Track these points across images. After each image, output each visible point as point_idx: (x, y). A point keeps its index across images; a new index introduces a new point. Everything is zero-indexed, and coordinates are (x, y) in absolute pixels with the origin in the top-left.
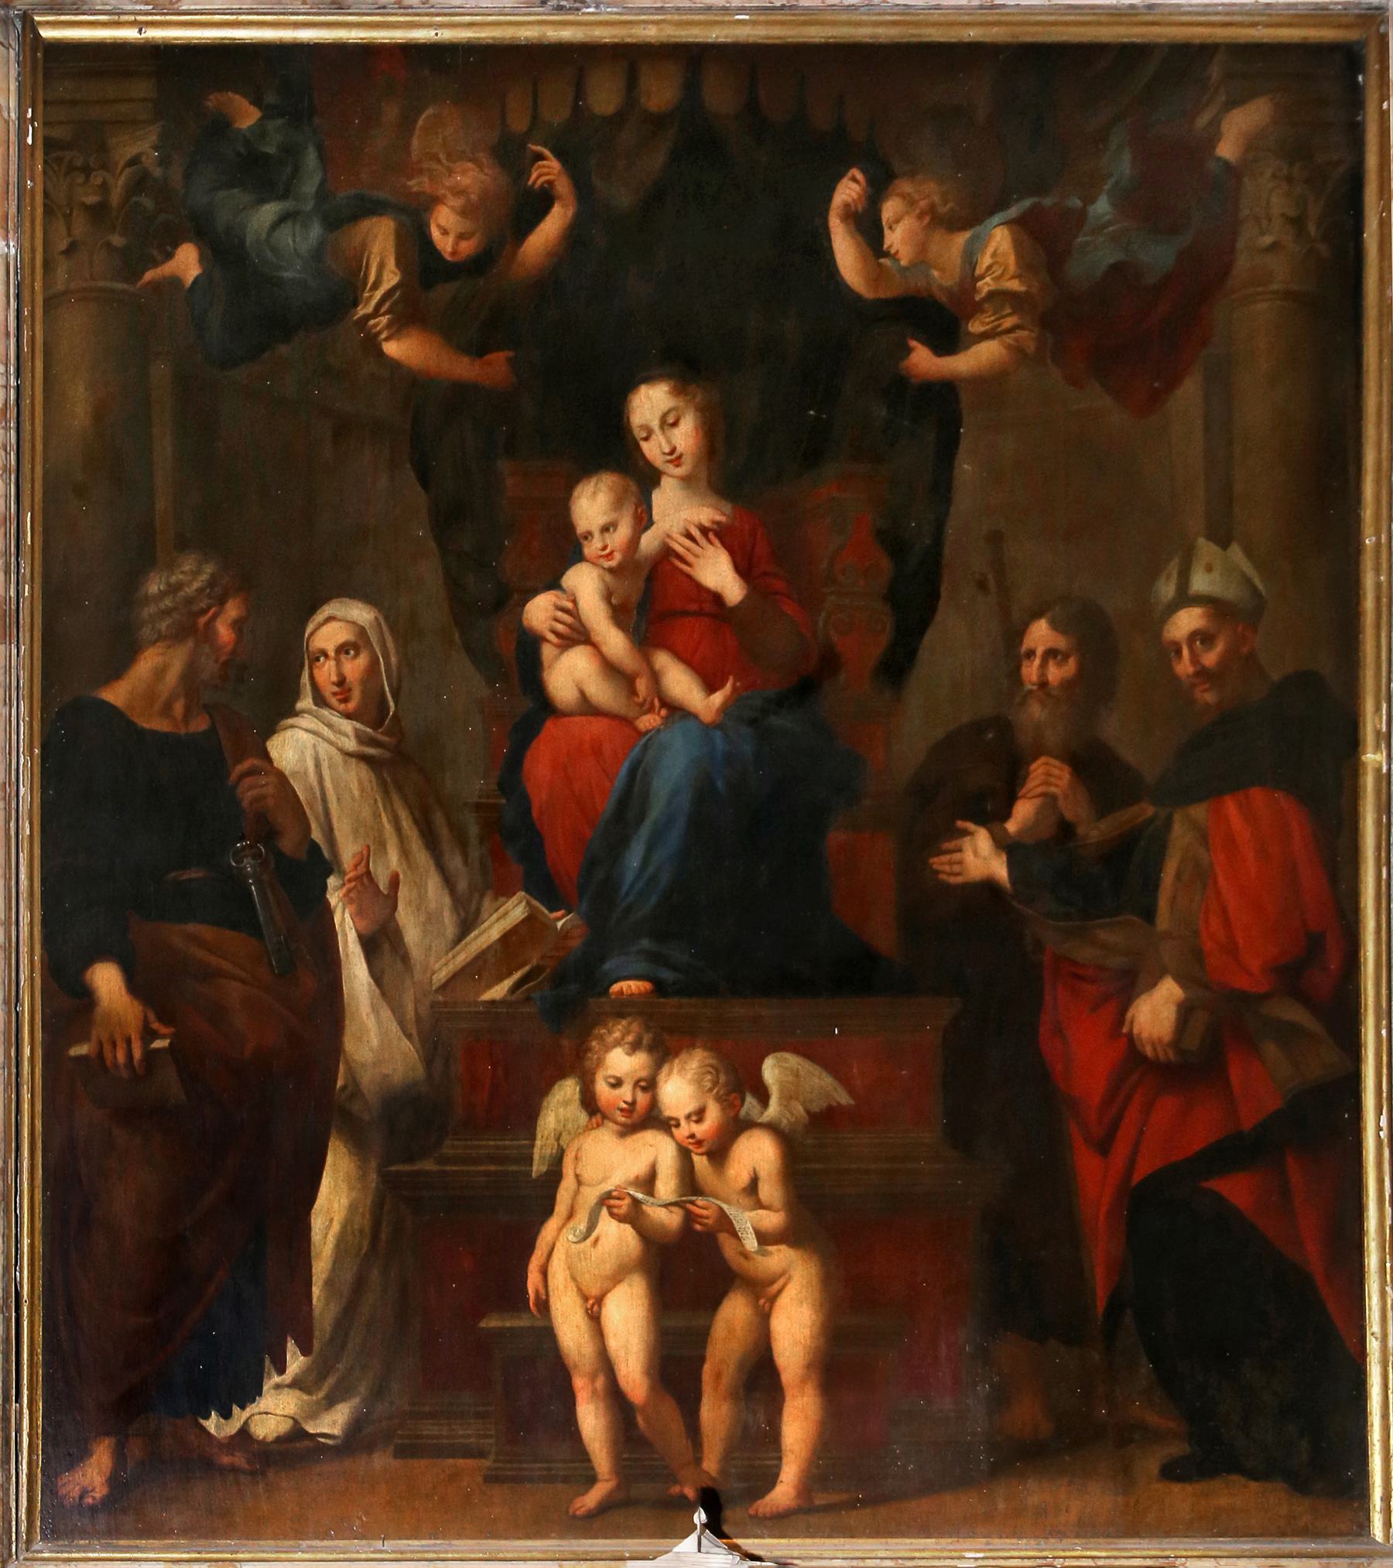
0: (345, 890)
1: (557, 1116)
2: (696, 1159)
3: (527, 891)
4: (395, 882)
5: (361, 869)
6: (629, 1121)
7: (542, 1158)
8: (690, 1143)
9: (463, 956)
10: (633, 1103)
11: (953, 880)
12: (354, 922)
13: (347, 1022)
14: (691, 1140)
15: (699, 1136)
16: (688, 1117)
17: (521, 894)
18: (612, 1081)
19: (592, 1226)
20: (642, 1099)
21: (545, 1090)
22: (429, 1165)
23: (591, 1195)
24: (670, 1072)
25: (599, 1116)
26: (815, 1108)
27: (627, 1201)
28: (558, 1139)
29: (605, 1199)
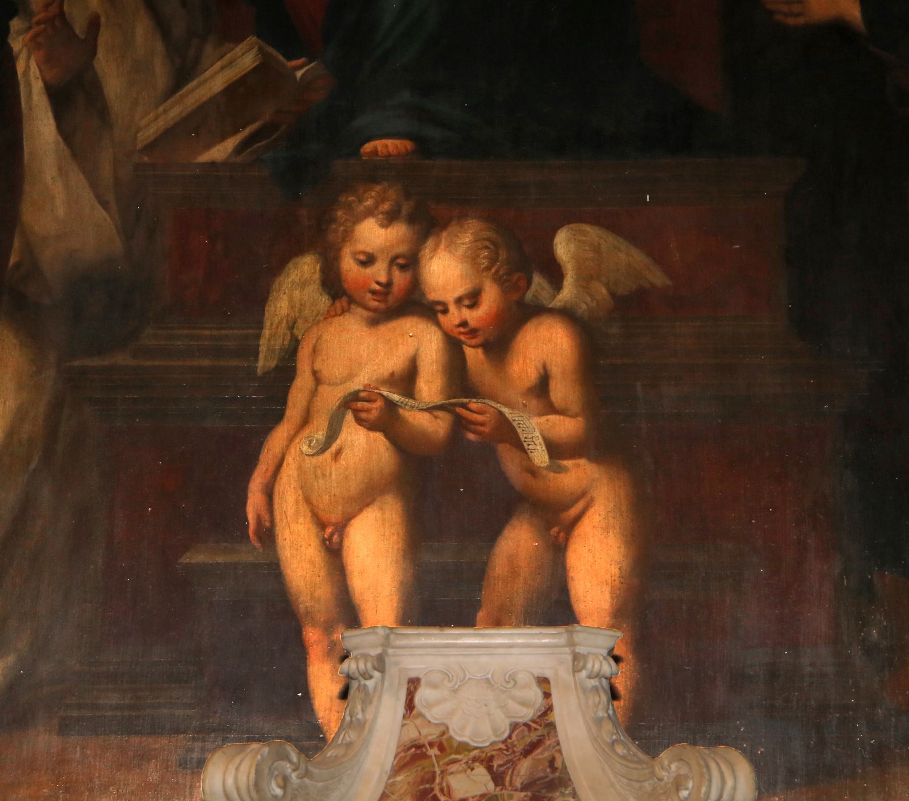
0: (31, 33)
1: (291, 300)
2: (469, 352)
3: (259, 37)
4: (94, 24)
5: (53, 9)
6: (382, 306)
7: (271, 350)
8: (461, 333)
9: (175, 111)
10: (388, 285)
11: (791, 21)
12: (40, 70)
13: (27, 188)
14: (462, 330)
15: (472, 323)
16: (459, 301)
17: (252, 39)
18: (362, 257)
19: (333, 433)
20: (400, 279)
21: (279, 266)
22: (122, 359)
23: (331, 397)
24: (435, 250)
25: (344, 300)
26: (621, 291)
27: (379, 404)
28: (291, 328)
29: (351, 402)
